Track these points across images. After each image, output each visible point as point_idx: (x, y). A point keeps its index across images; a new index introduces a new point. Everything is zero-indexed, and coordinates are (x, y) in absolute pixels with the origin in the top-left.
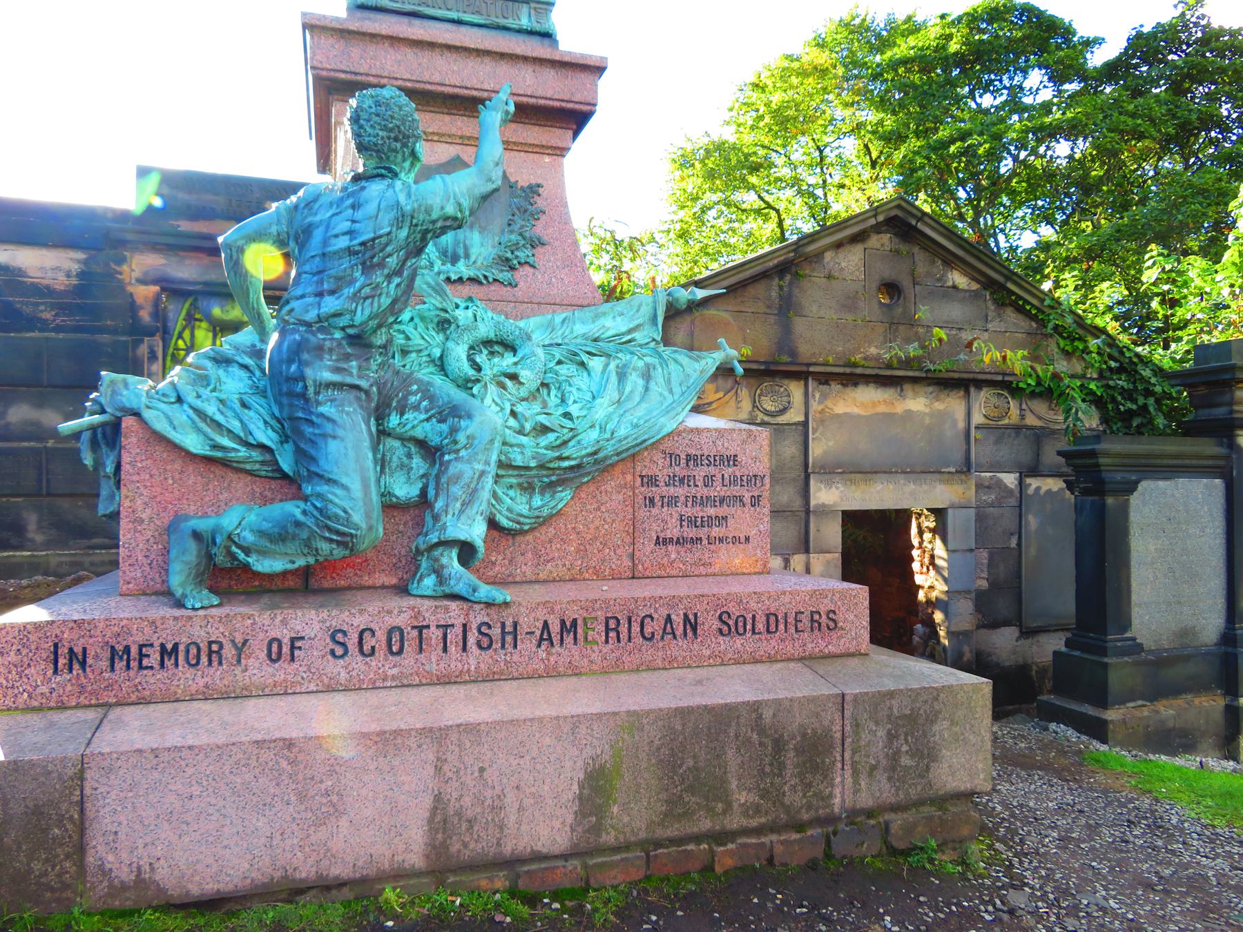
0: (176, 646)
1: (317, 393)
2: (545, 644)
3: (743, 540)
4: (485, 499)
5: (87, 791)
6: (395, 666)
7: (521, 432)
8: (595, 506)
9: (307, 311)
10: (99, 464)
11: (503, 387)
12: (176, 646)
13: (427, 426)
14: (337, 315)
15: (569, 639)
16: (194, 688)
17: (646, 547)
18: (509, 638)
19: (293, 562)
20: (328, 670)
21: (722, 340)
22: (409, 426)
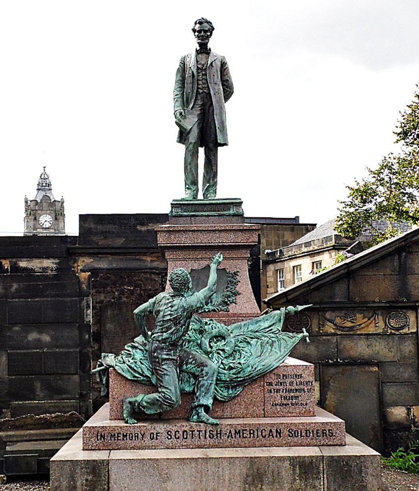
0: (127, 434)
1: (162, 362)
3: (305, 404)
5: (110, 469)
10: (101, 380)
11: (219, 353)
12: (127, 434)
13: (194, 369)
14: (167, 338)
18: (219, 435)
19: (156, 411)
21: (304, 329)
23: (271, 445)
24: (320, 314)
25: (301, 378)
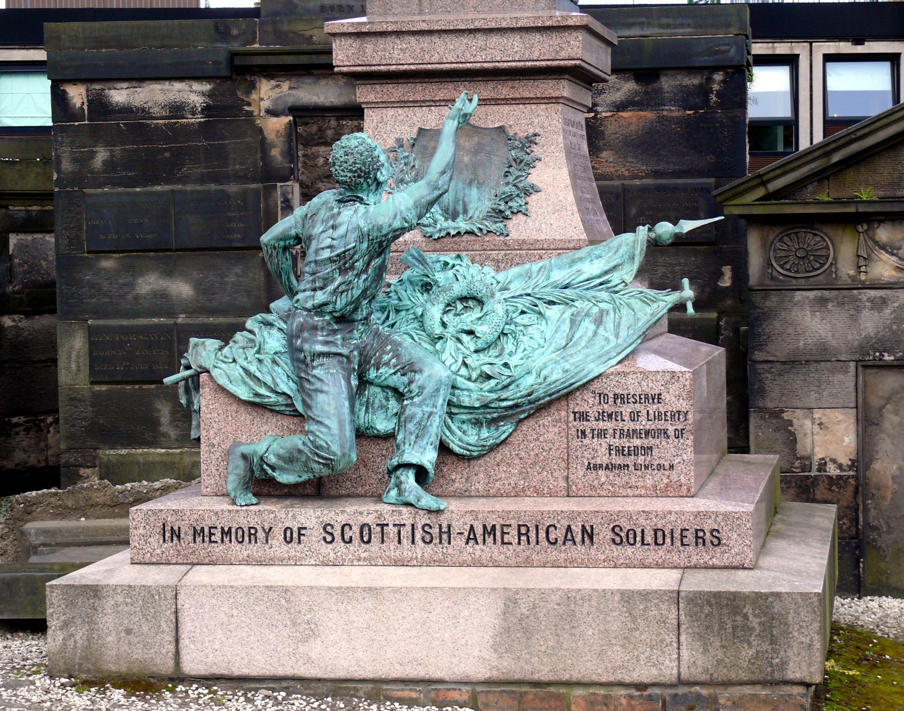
0: (230, 528)
1: (313, 361)
2: (472, 542)
3: (667, 467)
4: (433, 433)
5: (179, 607)
6: (365, 551)
7: (469, 379)
9: (307, 302)
11: (459, 340)
12: (230, 528)
13: (395, 377)
14: (325, 304)
15: (490, 540)
16: (241, 557)
17: (579, 472)
18: (445, 536)
20: (322, 551)
21: (686, 281)
22: (383, 378)
23: (571, 563)
24: (861, 230)
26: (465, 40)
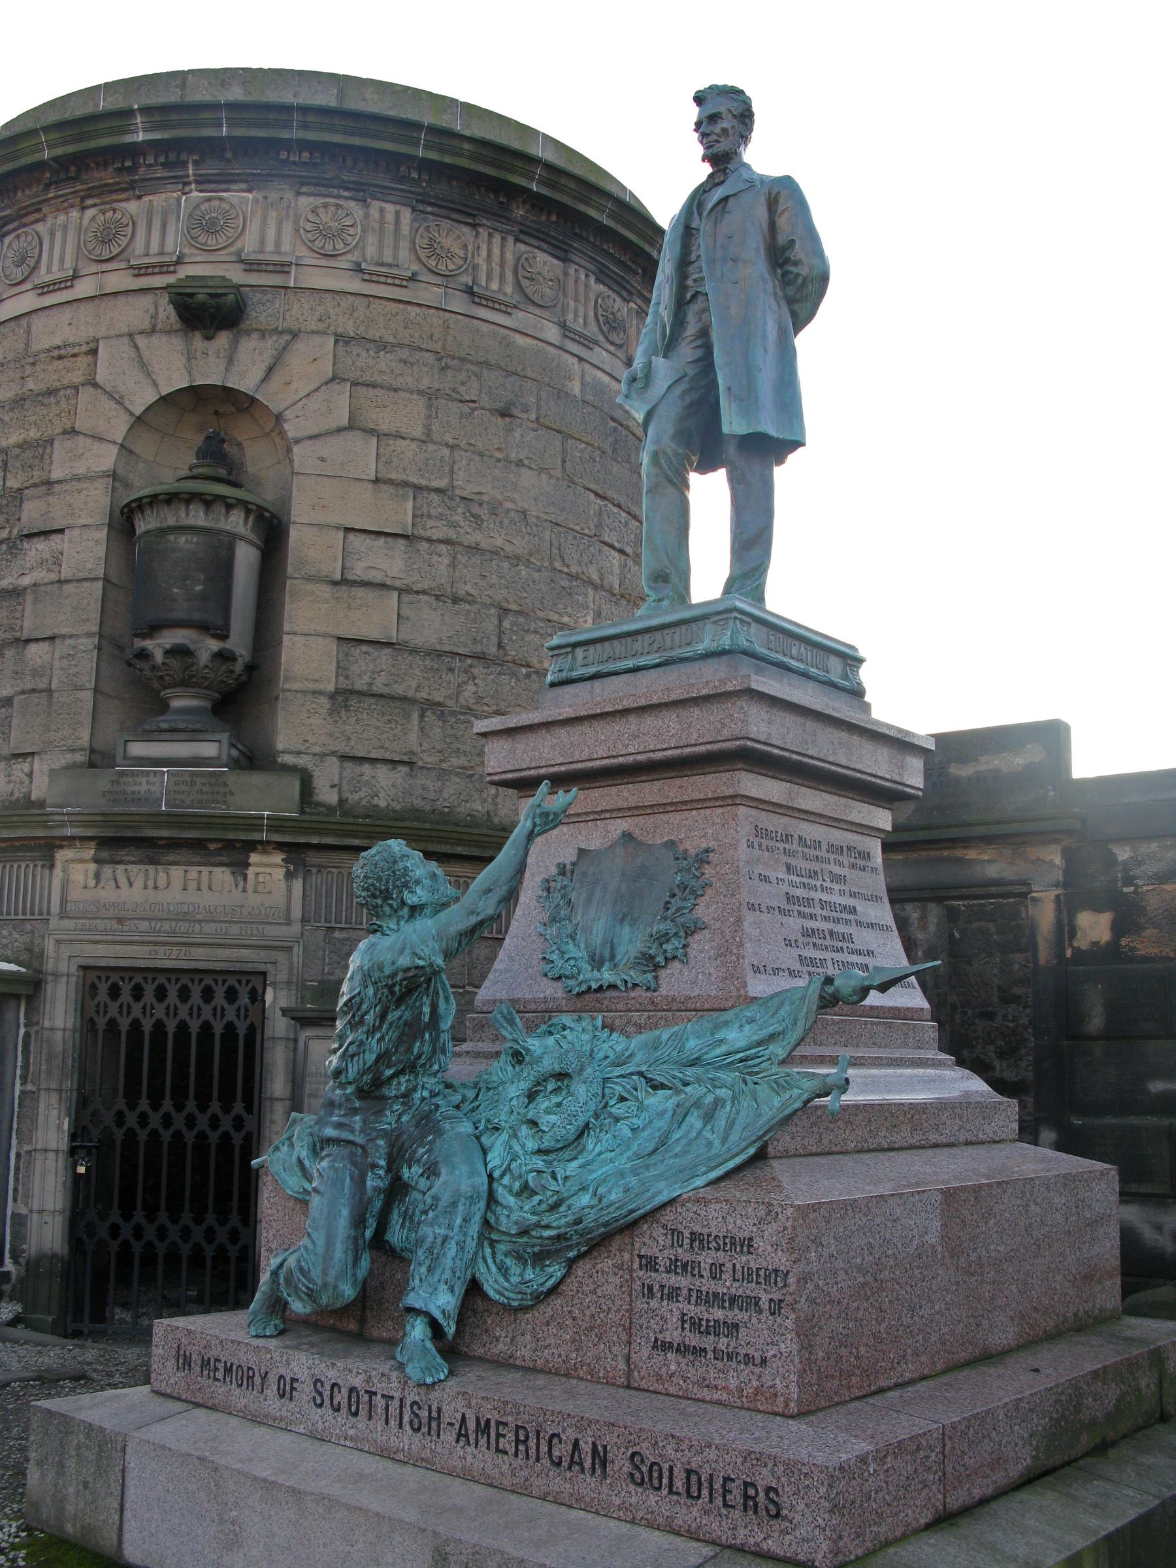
0: (232, 1364)
1: (322, 1149)
3: (758, 1361)
6: (352, 1427)
7: (510, 1191)
8: (592, 1287)
12: (232, 1364)
15: (483, 1442)
18: (434, 1424)
25: (750, 1253)
26: (618, 726)
